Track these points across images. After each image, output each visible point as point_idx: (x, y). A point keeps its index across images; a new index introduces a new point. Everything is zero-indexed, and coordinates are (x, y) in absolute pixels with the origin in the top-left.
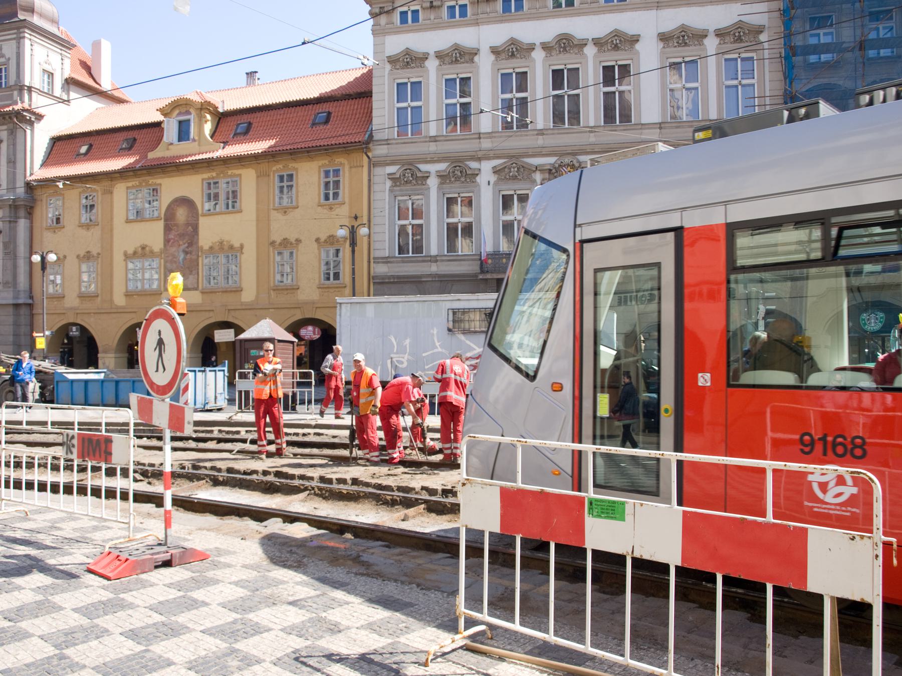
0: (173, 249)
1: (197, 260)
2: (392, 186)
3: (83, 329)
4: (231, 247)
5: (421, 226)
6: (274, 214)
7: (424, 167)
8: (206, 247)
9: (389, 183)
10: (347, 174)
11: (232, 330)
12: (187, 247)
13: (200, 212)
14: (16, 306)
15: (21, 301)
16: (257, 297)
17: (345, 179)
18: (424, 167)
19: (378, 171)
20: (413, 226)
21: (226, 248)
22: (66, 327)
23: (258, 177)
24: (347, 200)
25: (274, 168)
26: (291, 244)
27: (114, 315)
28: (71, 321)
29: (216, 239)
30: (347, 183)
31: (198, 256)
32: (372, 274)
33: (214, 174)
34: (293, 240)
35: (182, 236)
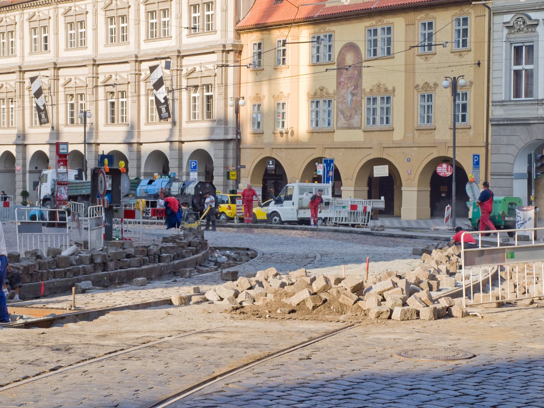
0: (344, 91)
1: (361, 101)
2: (510, 33)
3: (278, 164)
4: (386, 90)
5: (532, 70)
6: (418, 59)
7: (534, 15)
8: (368, 90)
9: (506, 31)
10: (473, 23)
11: (387, 166)
12: (354, 90)
13: (363, 58)
14: (228, 141)
15: (230, 137)
16: (405, 135)
17: (471, 26)
18: (534, 15)
19: (498, 20)
20: (526, 70)
21: (382, 90)
22: (266, 160)
23: (407, 25)
24: (473, 48)
25: (419, 17)
26: (431, 88)
27: (299, 150)
28: (268, 155)
29: (375, 82)
30: (473, 31)
31: (362, 98)
32: (490, 117)
33: (374, 22)
34: (432, 85)
35: (350, 78)
